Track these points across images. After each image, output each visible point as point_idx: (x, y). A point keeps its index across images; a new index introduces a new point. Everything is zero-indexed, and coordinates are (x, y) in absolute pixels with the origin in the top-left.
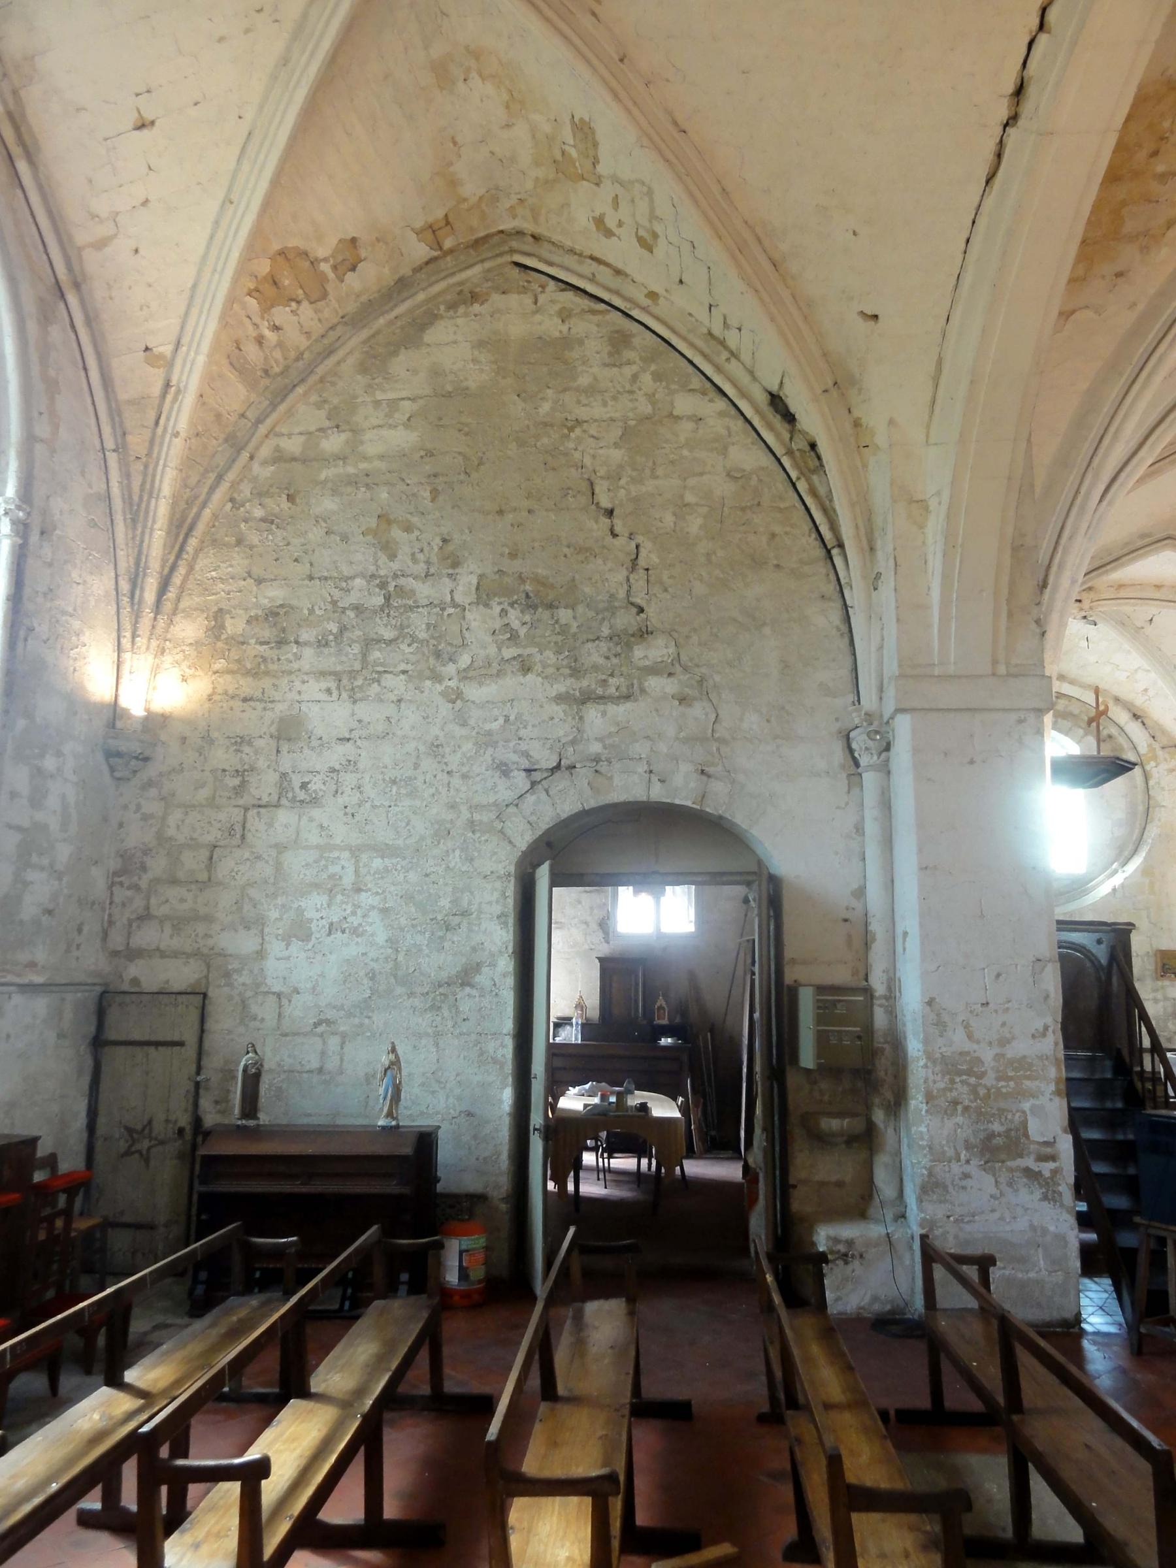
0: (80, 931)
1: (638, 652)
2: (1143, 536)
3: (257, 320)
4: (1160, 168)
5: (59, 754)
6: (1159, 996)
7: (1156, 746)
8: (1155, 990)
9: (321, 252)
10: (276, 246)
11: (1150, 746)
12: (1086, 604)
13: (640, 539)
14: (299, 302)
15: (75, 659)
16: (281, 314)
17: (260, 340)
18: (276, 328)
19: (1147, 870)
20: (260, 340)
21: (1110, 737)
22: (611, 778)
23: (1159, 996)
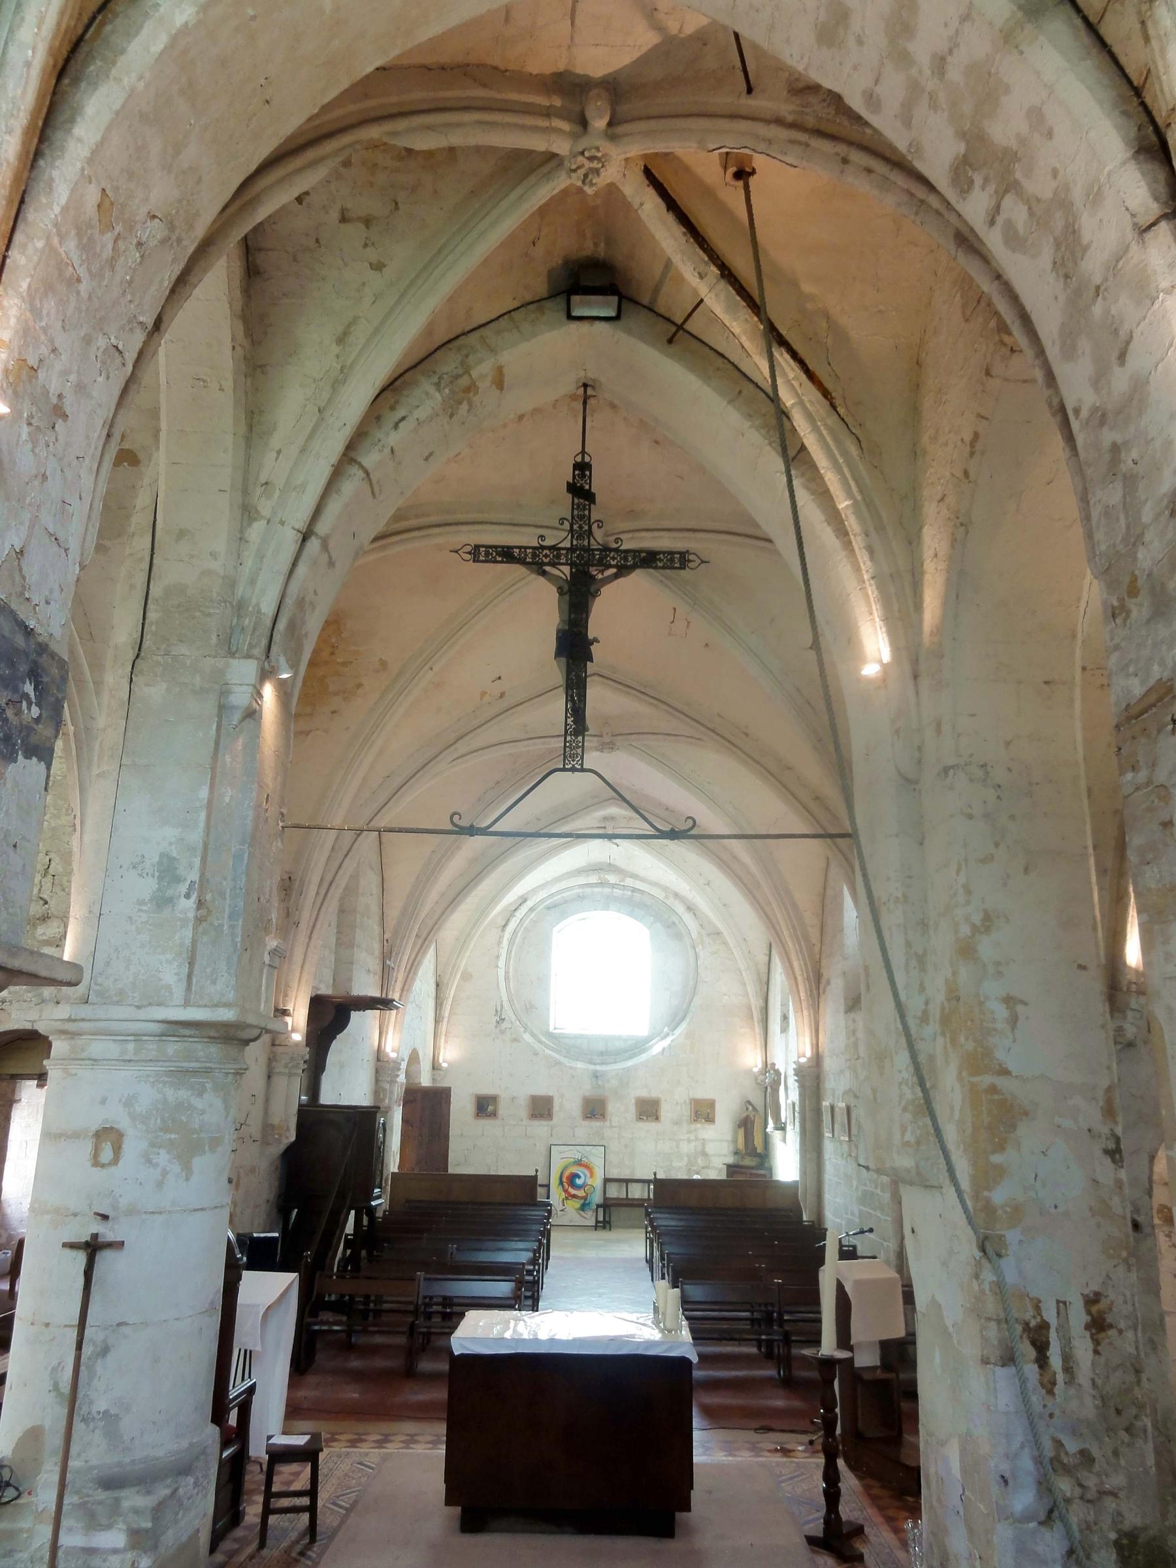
1: (40, 930)
4: (340, 660)
8: (689, 1132)
13: (52, 855)
19: (689, 1035)
22: (9, 1014)
23: (692, 1137)
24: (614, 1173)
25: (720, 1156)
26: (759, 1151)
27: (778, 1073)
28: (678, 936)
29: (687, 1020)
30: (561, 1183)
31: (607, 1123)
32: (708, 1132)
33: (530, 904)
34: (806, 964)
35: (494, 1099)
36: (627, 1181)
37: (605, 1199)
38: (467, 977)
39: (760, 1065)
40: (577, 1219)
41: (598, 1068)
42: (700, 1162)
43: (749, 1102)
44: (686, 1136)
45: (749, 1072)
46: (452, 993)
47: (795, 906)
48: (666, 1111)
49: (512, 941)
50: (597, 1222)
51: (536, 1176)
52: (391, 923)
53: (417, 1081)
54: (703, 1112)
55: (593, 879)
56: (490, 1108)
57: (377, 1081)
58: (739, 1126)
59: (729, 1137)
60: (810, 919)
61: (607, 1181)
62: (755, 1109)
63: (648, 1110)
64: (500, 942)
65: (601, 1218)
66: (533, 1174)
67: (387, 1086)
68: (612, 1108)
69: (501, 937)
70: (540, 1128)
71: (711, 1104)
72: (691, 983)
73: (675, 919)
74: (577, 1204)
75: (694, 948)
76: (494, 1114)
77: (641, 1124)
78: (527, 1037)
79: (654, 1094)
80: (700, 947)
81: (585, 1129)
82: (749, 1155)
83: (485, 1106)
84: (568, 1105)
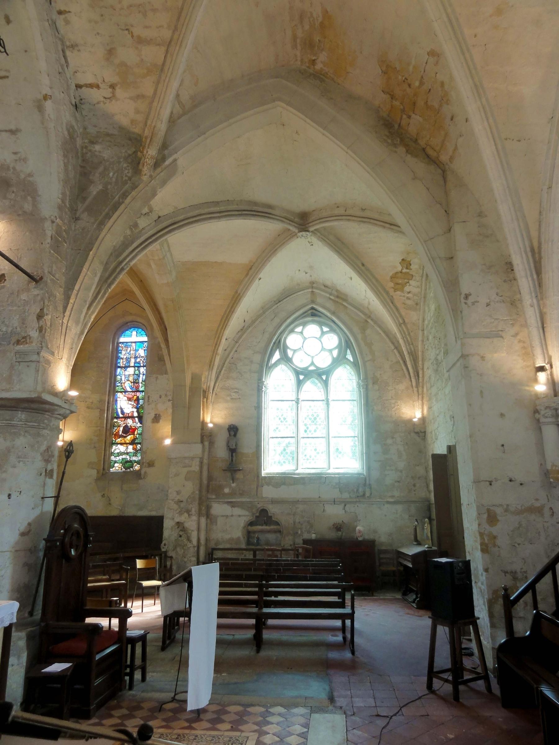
0: (414, 485)
3: (403, 295)
4: (417, 84)
5: (393, 438)
9: (399, 269)
10: (388, 278)
14: (408, 282)
15: (395, 411)
16: (407, 289)
17: (408, 298)
18: (409, 293)
20: (408, 298)
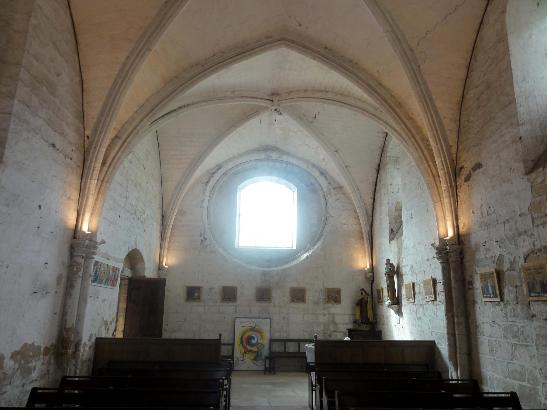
2: (267, 37)
6: (326, 312)
7: (331, 188)
8: (325, 309)
11: (328, 187)
12: (275, 102)
19: (323, 248)
21: (312, 184)
23: (326, 312)
24: (276, 336)
25: (343, 324)
26: (371, 320)
27: (392, 265)
28: (315, 191)
29: (322, 240)
30: (242, 342)
31: (272, 304)
32: (336, 309)
33: (223, 170)
34: (446, 161)
35: (199, 289)
36: (285, 341)
37: (271, 352)
38: (182, 213)
39: (368, 266)
40: (253, 367)
41: (266, 269)
42: (332, 328)
43: (363, 289)
44: (322, 312)
45: (362, 271)
46: (172, 221)
47: (436, 112)
48: (310, 296)
49: (212, 193)
50: (265, 367)
51: (220, 339)
52: (91, 122)
53: (142, 275)
54: (333, 296)
55: (263, 156)
56: (196, 295)
57: (72, 256)
58: (357, 305)
59: (349, 312)
60: (449, 125)
61: (272, 341)
62: (367, 294)
63: (298, 295)
64: (204, 193)
65: (268, 366)
66: (218, 337)
67: (82, 261)
68: (275, 294)
69: (205, 189)
70: (229, 308)
71: (338, 291)
72: (323, 218)
73: (313, 181)
74: (252, 357)
75: (325, 197)
76: (198, 299)
77: (293, 305)
78: (220, 250)
79: (301, 285)
80: (329, 196)
81: (257, 308)
82: (364, 323)
83: (193, 293)
84: (246, 293)
